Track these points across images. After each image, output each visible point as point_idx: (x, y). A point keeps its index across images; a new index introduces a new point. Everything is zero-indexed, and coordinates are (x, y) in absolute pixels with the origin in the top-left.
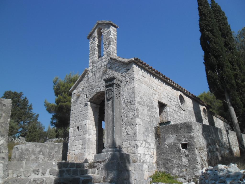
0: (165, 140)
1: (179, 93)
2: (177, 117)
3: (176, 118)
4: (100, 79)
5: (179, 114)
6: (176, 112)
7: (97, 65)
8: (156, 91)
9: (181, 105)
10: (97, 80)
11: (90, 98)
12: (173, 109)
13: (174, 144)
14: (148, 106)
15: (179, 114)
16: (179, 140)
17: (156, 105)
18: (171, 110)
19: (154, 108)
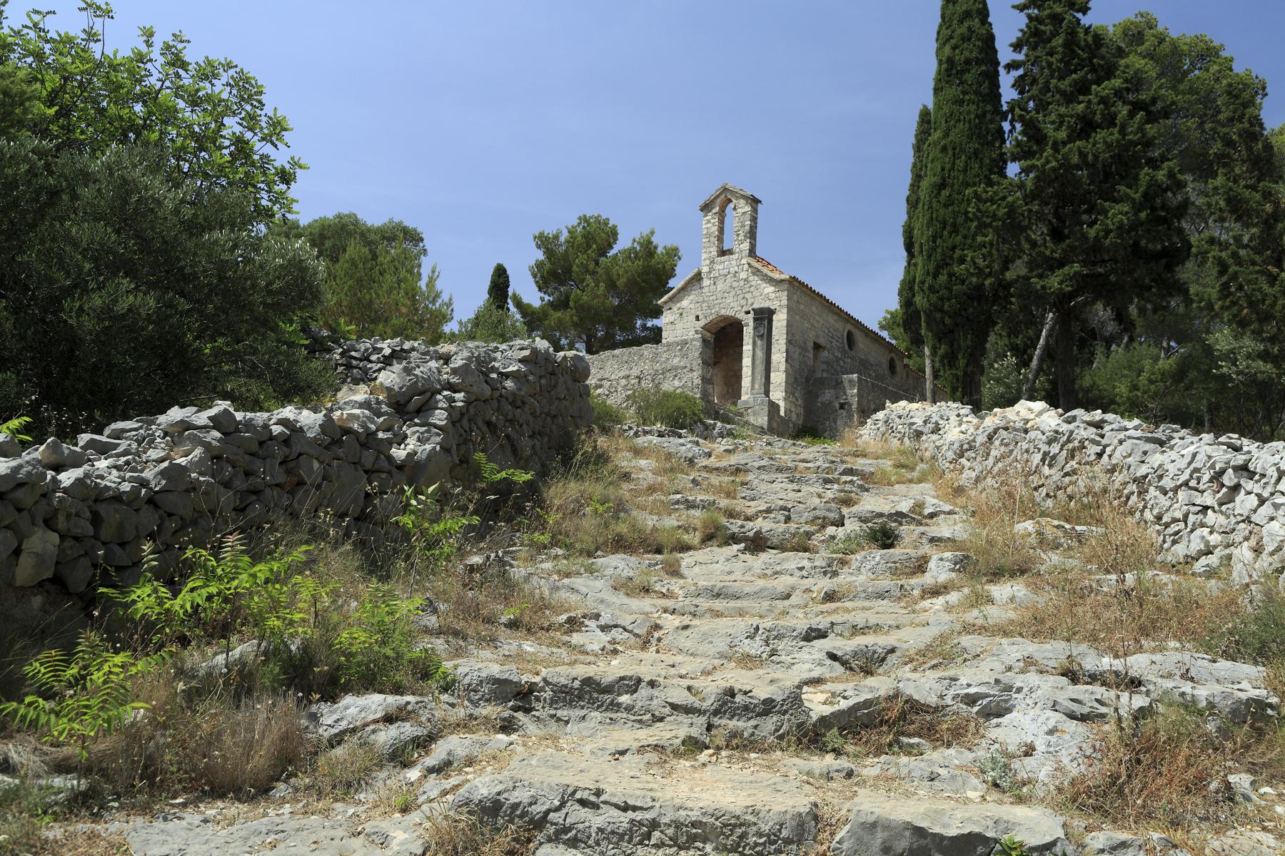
0: (817, 397)
1: (849, 327)
2: (839, 368)
3: (836, 370)
4: (726, 295)
5: (841, 363)
6: (838, 360)
7: (721, 267)
8: (812, 324)
9: (847, 348)
10: (719, 296)
11: (703, 322)
12: (833, 354)
13: (830, 402)
14: (800, 347)
15: (841, 363)
16: (837, 398)
17: (810, 345)
18: (831, 356)
19: (807, 350)
